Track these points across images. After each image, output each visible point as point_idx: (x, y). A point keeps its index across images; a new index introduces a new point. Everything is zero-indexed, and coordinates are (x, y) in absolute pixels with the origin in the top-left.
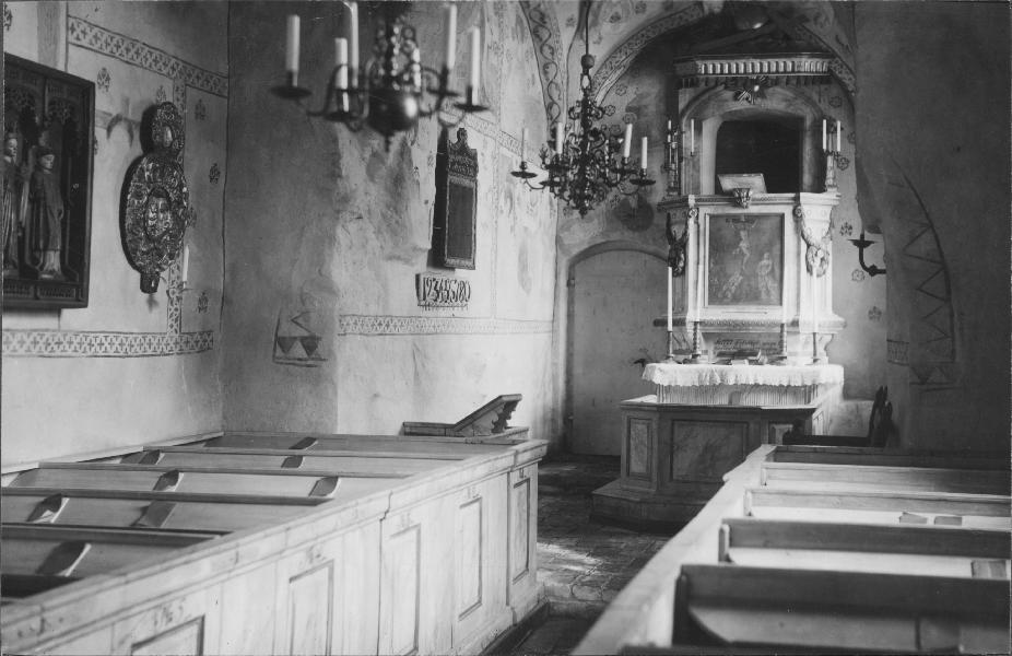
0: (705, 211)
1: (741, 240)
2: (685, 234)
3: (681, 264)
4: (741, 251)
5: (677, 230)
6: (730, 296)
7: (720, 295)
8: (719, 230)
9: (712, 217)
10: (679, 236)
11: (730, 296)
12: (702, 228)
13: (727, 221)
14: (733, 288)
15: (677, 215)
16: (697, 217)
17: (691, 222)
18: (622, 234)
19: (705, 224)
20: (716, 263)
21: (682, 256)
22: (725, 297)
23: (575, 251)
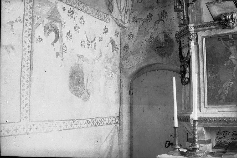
0: (201, 35)
1: (231, 54)
2: (189, 53)
3: (187, 75)
4: (231, 61)
5: (185, 51)
6: (224, 98)
7: (216, 98)
8: (213, 47)
9: (207, 38)
10: (186, 56)
11: (224, 98)
12: (200, 47)
13: (219, 40)
14: (227, 91)
15: (184, 41)
16: (197, 39)
17: (192, 44)
18: (156, 59)
19: (203, 44)
20: (212, 73)
21: (188, 69)
22: (220, 99)
23: (131, 72)
